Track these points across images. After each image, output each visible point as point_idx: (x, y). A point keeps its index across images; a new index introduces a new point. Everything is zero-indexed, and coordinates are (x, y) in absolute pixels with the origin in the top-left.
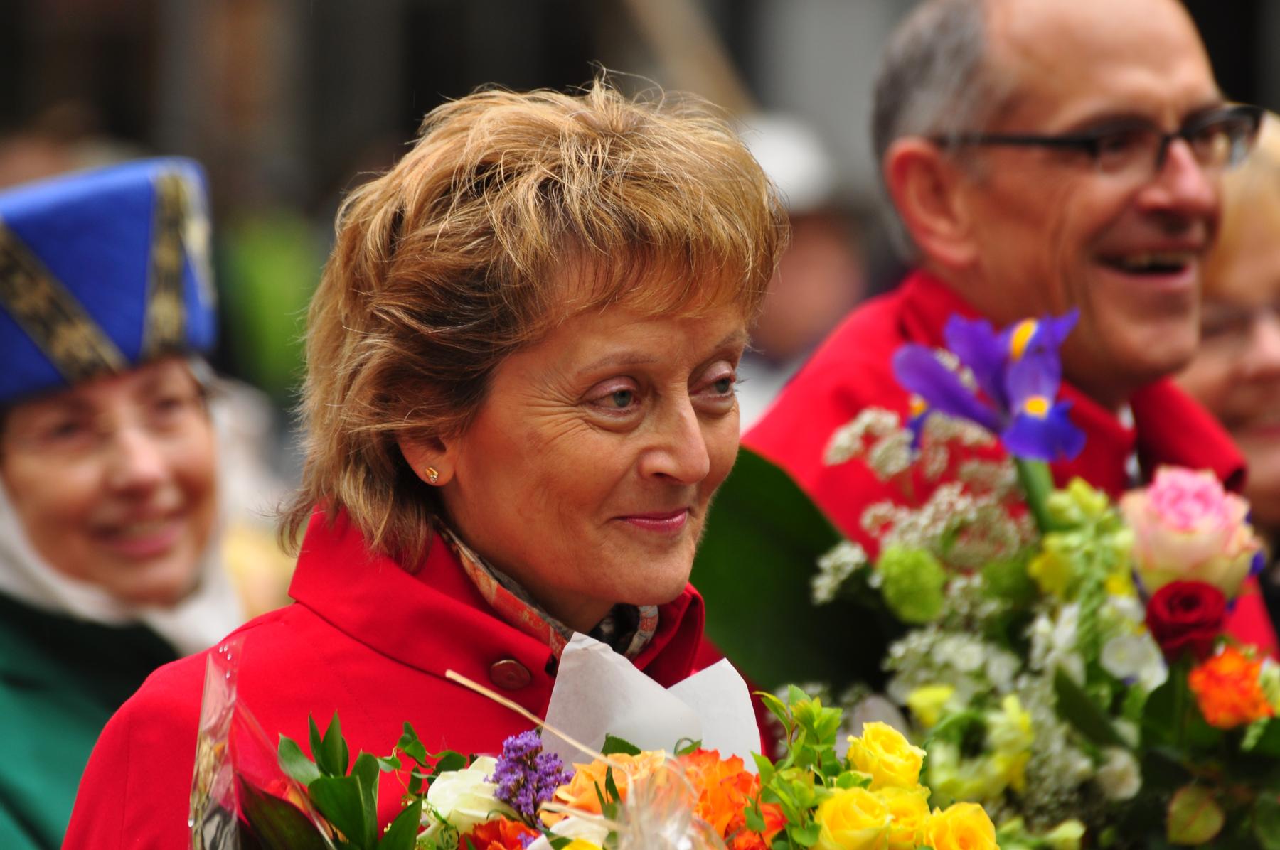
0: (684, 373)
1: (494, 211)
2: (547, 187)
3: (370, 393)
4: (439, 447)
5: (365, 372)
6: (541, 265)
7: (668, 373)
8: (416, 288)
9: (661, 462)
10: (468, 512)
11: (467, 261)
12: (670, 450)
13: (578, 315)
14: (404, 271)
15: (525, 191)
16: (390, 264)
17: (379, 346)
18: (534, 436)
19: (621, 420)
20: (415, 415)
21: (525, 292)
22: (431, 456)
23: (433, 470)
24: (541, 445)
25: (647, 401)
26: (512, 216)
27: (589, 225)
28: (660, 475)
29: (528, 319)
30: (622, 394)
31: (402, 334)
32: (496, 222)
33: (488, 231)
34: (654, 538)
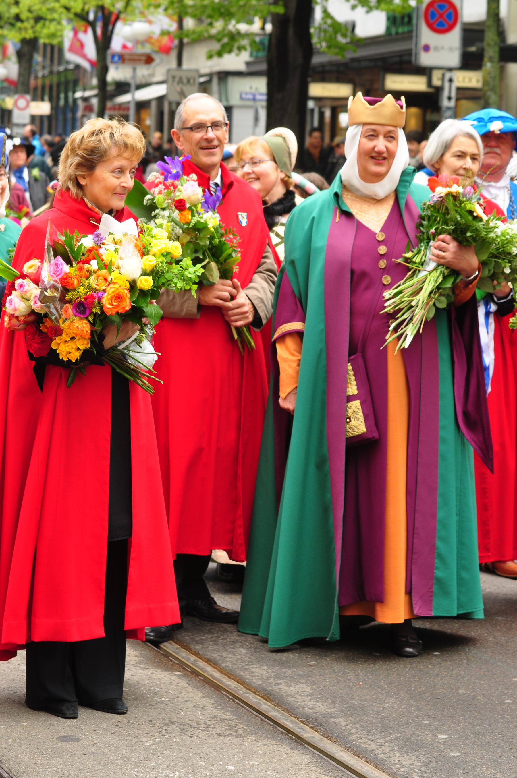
0: (129, 169)
1: (101, 137)
2: (111, 134)
3: (74, 167)
4: (85, 178)
5: (74, 164)
6: (110, 147)
7: (126, 169)
8: (86, 149)
9: (124, 184)
10: (88, 190)
11: (96, 146)
12: (126, 182)
13: (114, 157)
14: (83, 146)
15: (107, 135)
16: (81, 145)
17: (77, 160)
18: (103, 178)
19: (118, 176)
20: (83, 172)
21: (105, 152)
22: (83, 180)
23: (83, 182)
24: (104, 180)
25: (122, 173)
26: (105, 138)
27: (118, 142)
28: (123, 187)
29: (106, 156)
30: (119, 171)
31: (83, 157)
32: (102, 139)
33: (100, 140)
34: (120, 198)
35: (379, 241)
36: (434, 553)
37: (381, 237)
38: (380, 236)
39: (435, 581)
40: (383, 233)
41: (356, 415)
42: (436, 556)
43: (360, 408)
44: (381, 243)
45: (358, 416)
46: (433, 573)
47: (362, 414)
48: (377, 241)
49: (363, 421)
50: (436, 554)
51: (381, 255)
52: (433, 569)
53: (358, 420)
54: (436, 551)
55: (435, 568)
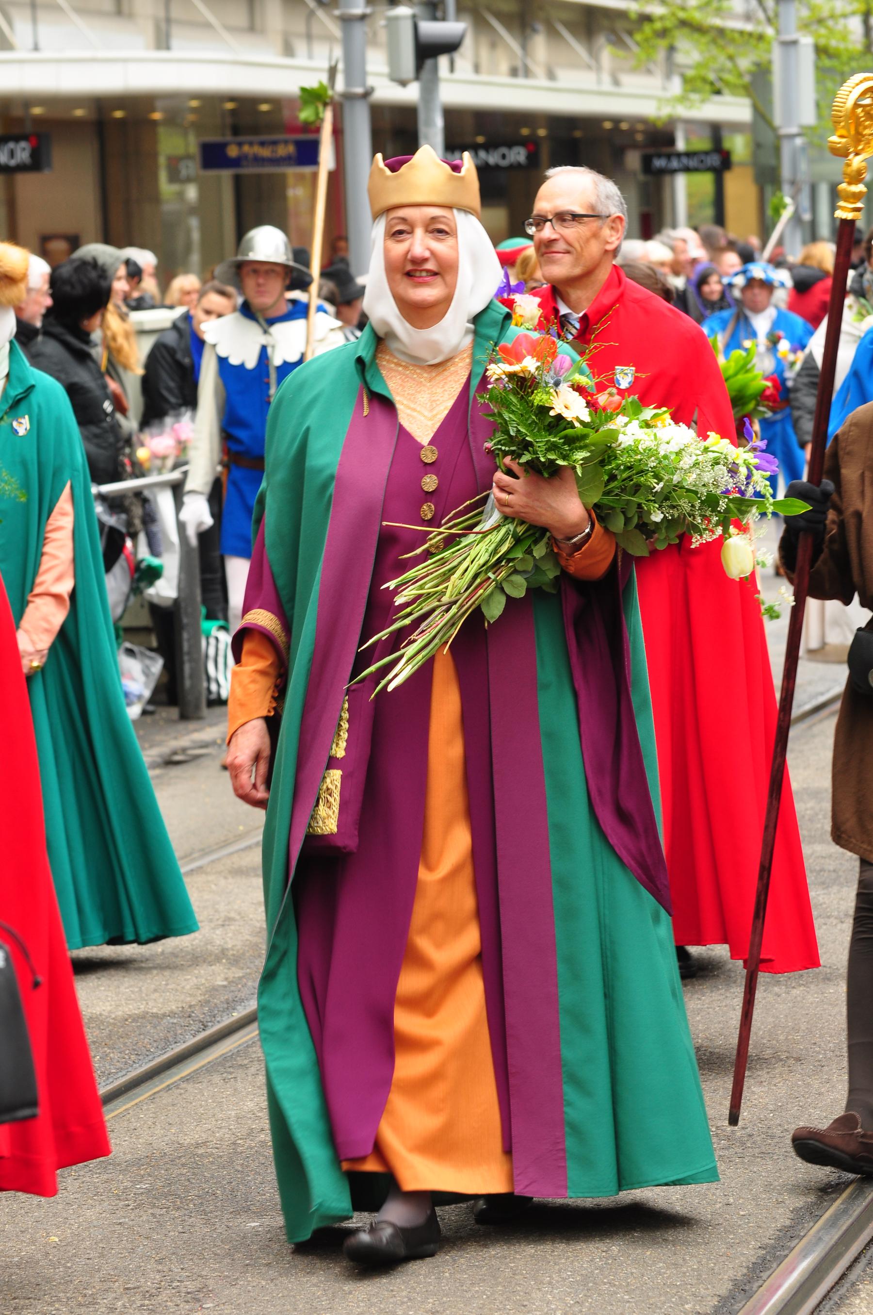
35: (426, 464)
36: (560, 1074)
37: (429, 456)
38: (429, 454)
39: (567, 1129)
40: (434, 448)
41: (328, 797)
42: (564, 1080)
43: (339, 785)
44: (428, 468)
45: (331, 799)
46: (563, 1112)
47: (338, 799)
48: (422, 465)
49: (337, 811)
50: (564, 1075)
51: (427, 493)
52: (562, 1105)
53: (329, 807)
54: (564, 1069)
55: (565, 1103)
